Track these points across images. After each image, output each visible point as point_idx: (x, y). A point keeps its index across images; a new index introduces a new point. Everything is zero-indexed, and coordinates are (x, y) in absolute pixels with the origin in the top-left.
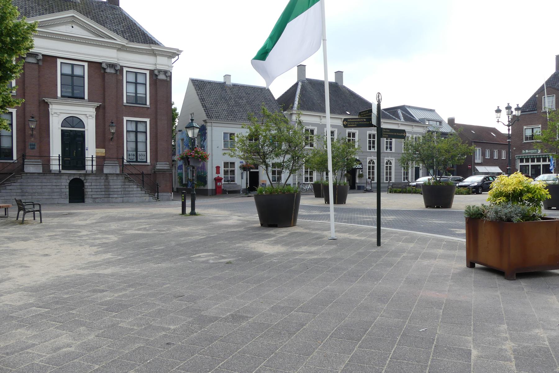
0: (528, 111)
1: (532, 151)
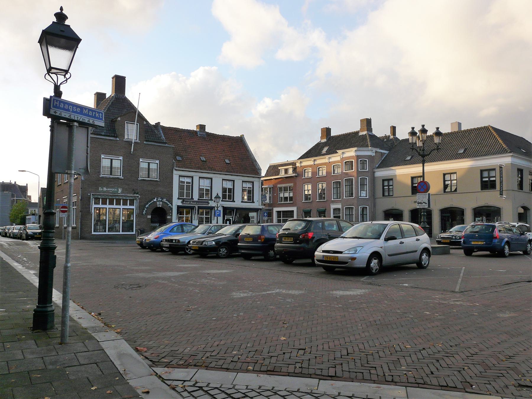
0: (104, 135)
1: (112, 189)
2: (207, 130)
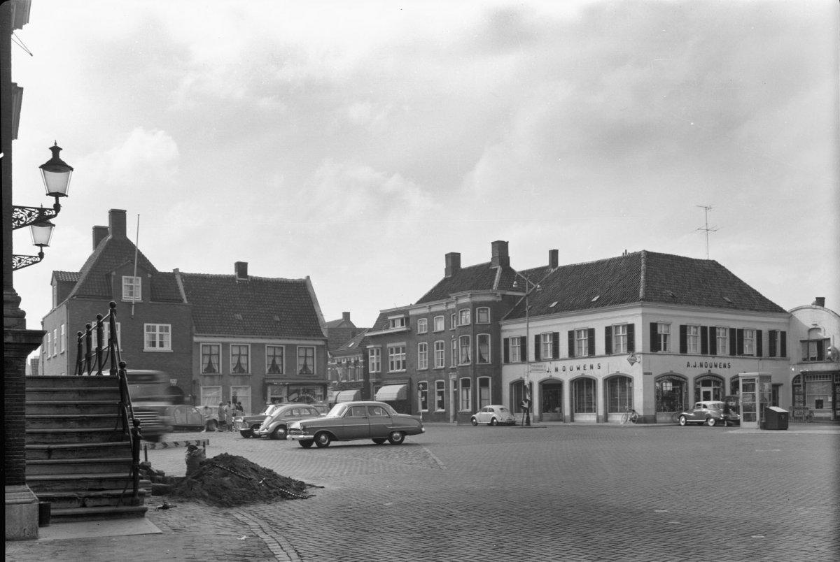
2: (252, 272)
